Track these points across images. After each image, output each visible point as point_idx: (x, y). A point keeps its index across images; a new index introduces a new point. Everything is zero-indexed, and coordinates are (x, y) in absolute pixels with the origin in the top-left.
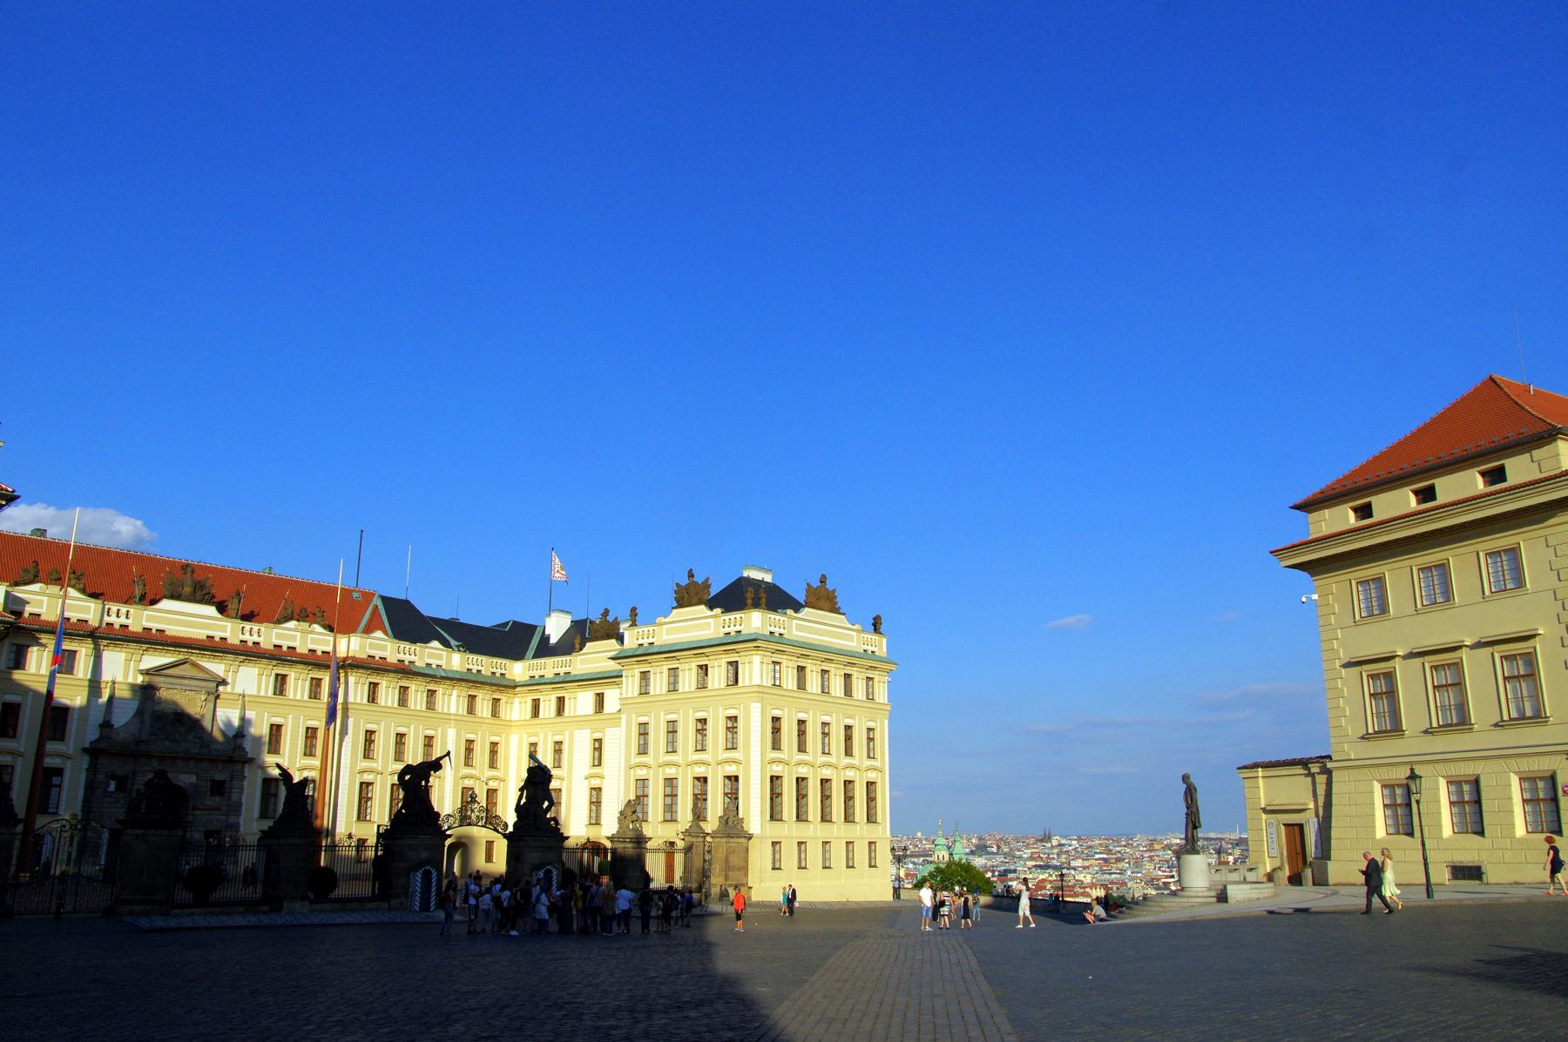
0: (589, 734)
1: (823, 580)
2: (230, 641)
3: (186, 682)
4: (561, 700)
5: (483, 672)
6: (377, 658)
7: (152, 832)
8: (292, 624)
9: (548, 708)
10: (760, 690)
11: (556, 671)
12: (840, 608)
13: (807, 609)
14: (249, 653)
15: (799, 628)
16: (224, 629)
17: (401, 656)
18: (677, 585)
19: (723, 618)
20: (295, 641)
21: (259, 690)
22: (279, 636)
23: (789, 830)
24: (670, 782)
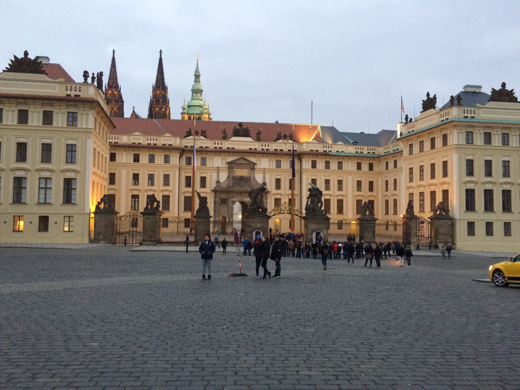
1: (504, 85)
2: (258, 149)
3: (243, 165)
4: (395, 162)
5: (364, 153)
6: (314, 151)
8: (280, 141)
9: (391, 165)
10: (458, 147)
11: (394, 149)
14: (265, 153)
15: (484, 113)
17: (325, 149)
18: (423, 101)
20: (282, 147)
21: (270, 166)
24: (422, 194)
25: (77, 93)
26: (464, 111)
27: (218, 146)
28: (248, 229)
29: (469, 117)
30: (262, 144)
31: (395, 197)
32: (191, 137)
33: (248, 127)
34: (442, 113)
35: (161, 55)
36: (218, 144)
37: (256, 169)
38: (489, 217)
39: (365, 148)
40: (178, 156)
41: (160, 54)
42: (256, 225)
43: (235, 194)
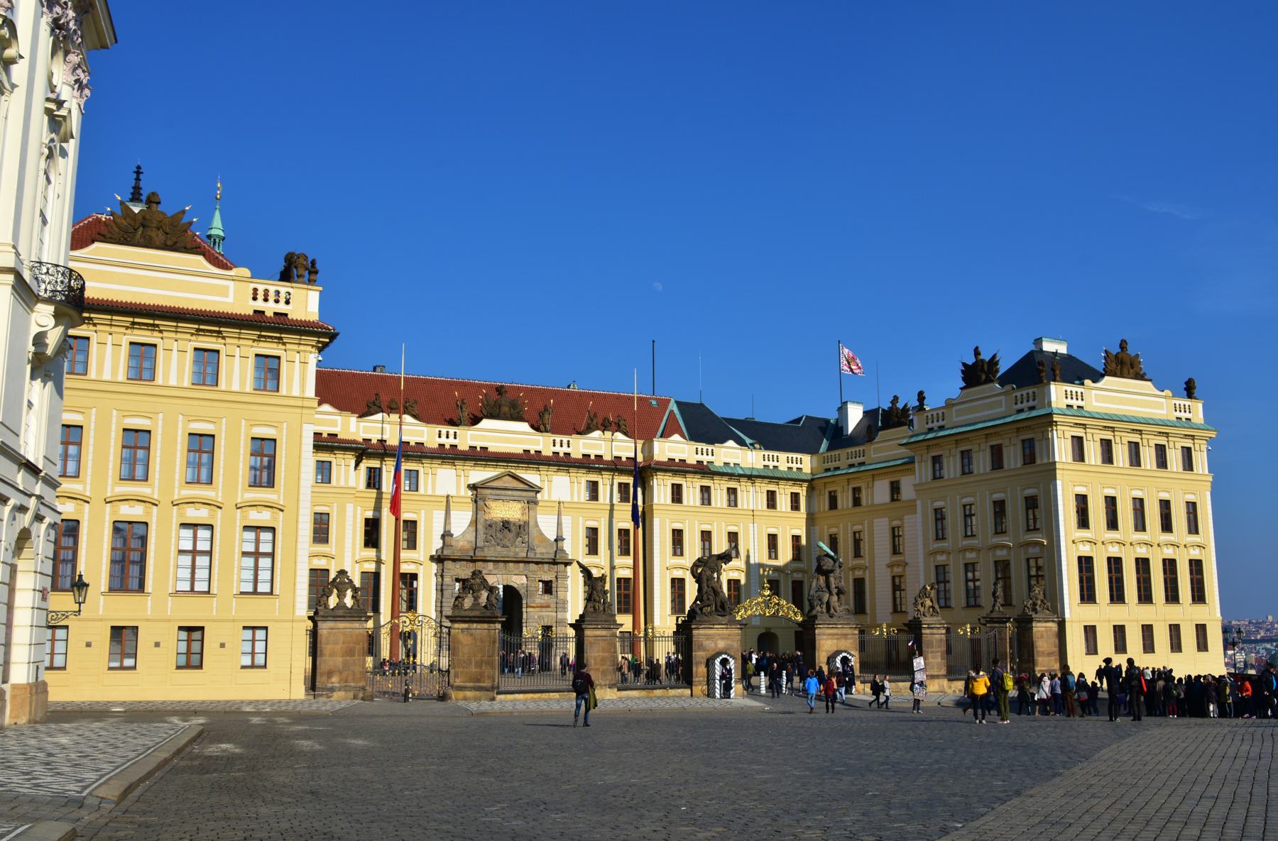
0: (887, 523)
1: (1123, 345)
2: (544, 453)
3: (510, 492)
4: (856, 490)
5: (780, 468)
6: (677, 461)
7: (475, 625)
8: (597, 434)
9: (845, 500)
12: (1145, 374)
13: (1106, 378)
14: (563, 463)
15: (1098, 399)
16: (538, 443)
17: (700, 457)
18: (964, 364)
19: (1014, 395)
22: (585, 446)
23: (1103, 614)
24: (970, 567)
25: (281, 308)
26: (1066, 394)
27: (448, 442)
28: (698, 653)
29: (1075, 408)
30: (554, 441)
31: (859, 574)
32: (379, 416)
33: (519, 397)
34: (1018, 394)
35: (138, 179)
36: (447, 437)
37: (540, 504)
38: (1118, 614)
39: (783, 456)
40: (353, 463)
41: (135, 176)
42: (716, 644)
43: (491, 565)
